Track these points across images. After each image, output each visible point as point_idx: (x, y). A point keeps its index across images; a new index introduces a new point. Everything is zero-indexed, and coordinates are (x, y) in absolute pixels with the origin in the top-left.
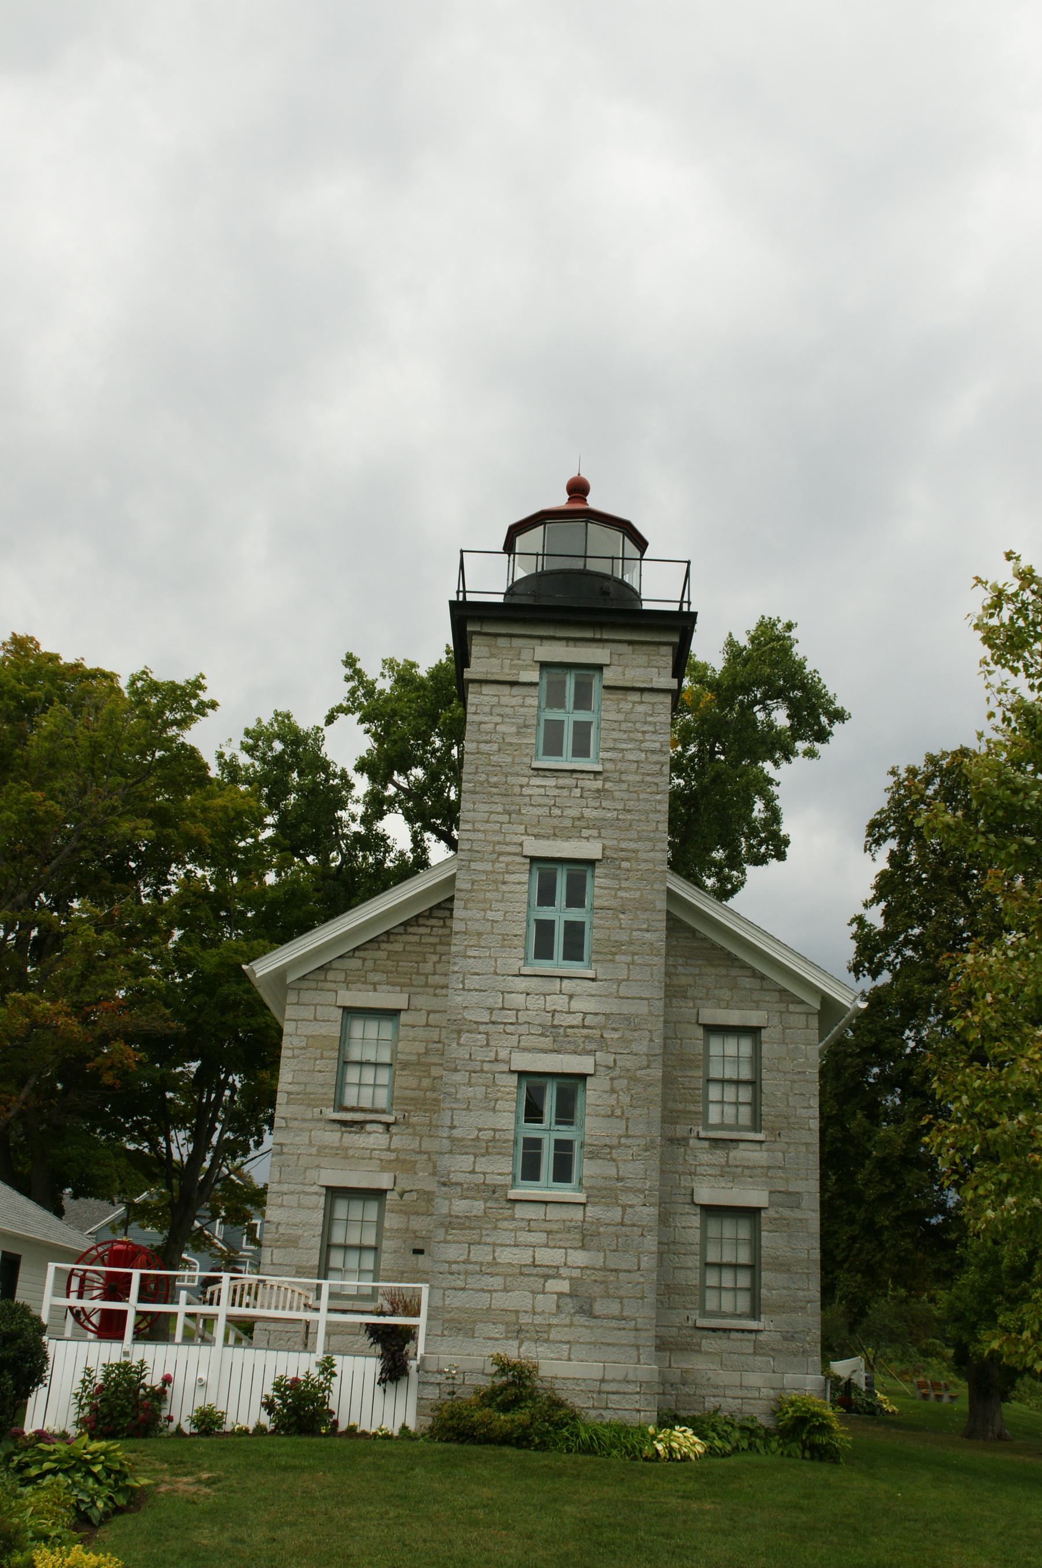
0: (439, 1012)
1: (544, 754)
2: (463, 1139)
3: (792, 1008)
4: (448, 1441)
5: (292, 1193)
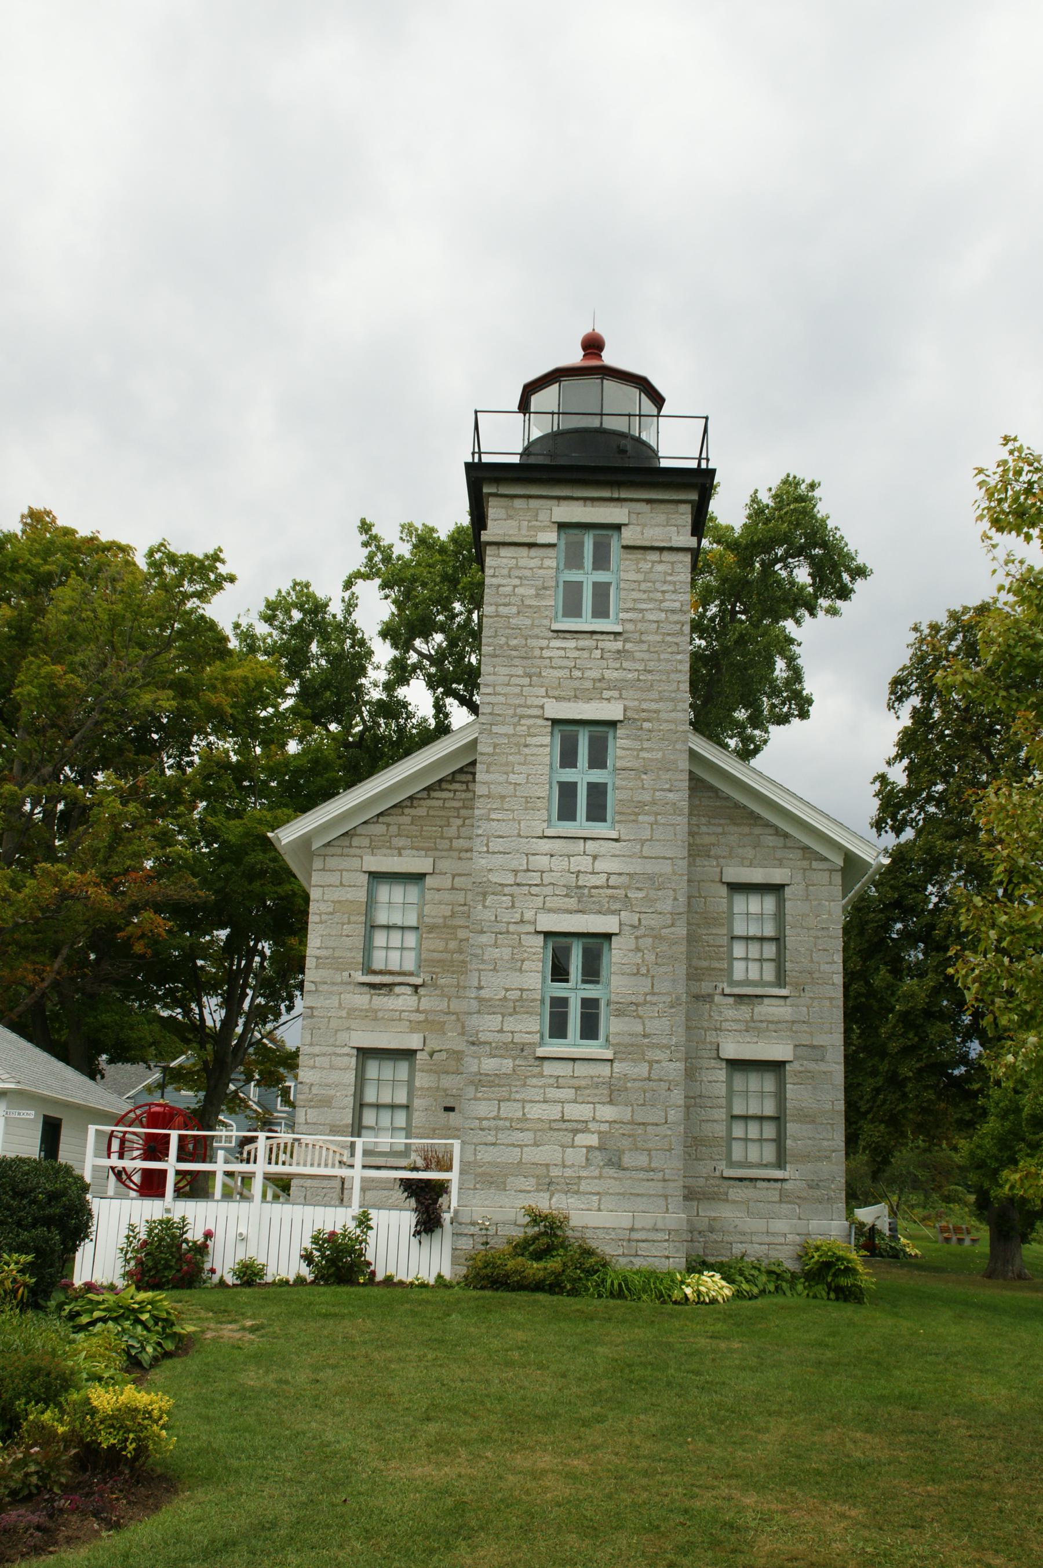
2: (490, 1000)
3: (815, 864)
4: (483, 1288)
5: (324, 1055)
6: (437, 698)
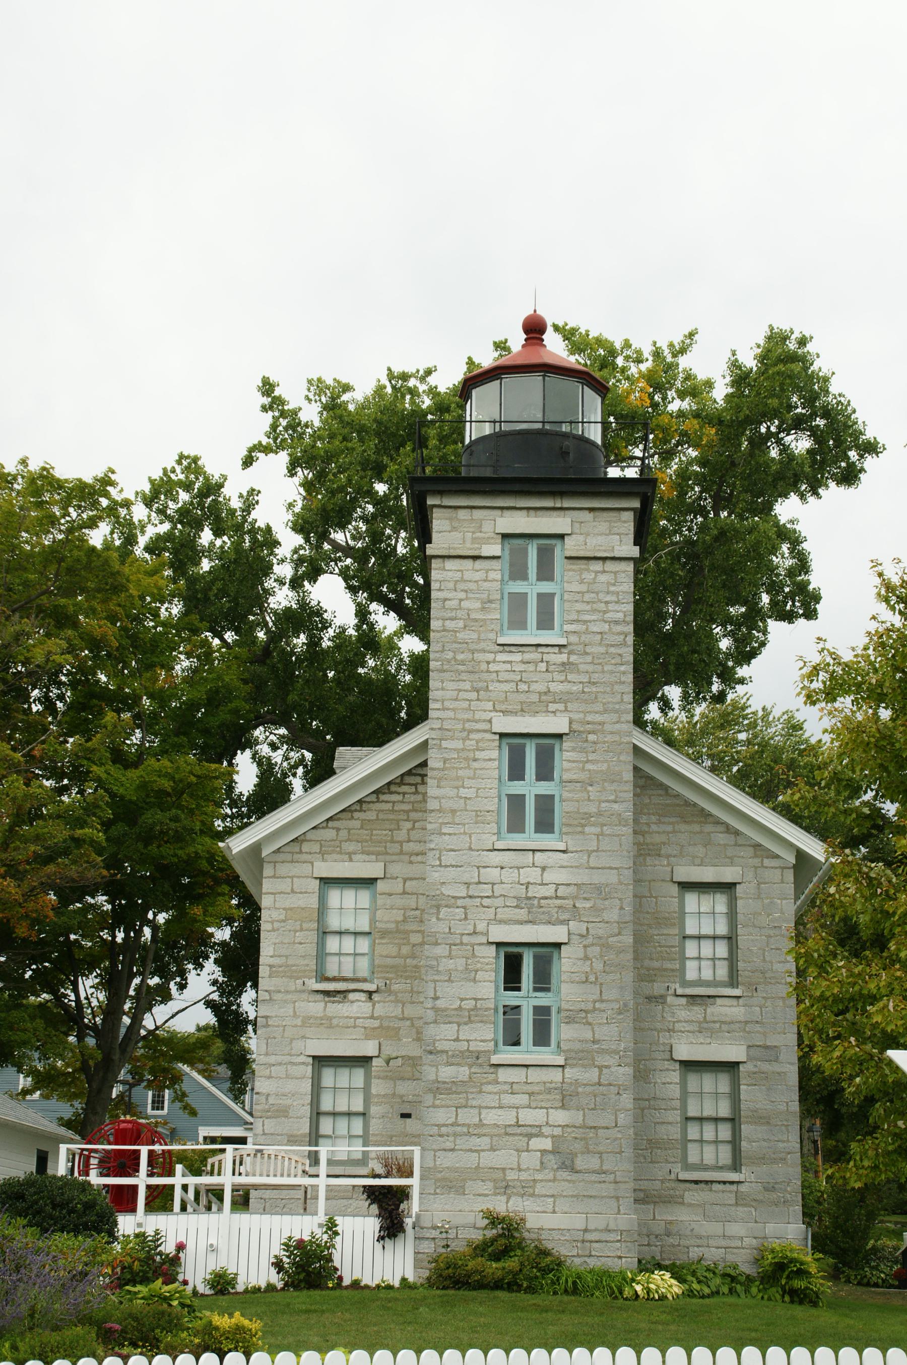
0: (416, 879)
1: (509, 629)
2: (446, 1009)
3: (767, 862)
4: (444, 1288)
5: (280, 1064)
6: (359, 605)
